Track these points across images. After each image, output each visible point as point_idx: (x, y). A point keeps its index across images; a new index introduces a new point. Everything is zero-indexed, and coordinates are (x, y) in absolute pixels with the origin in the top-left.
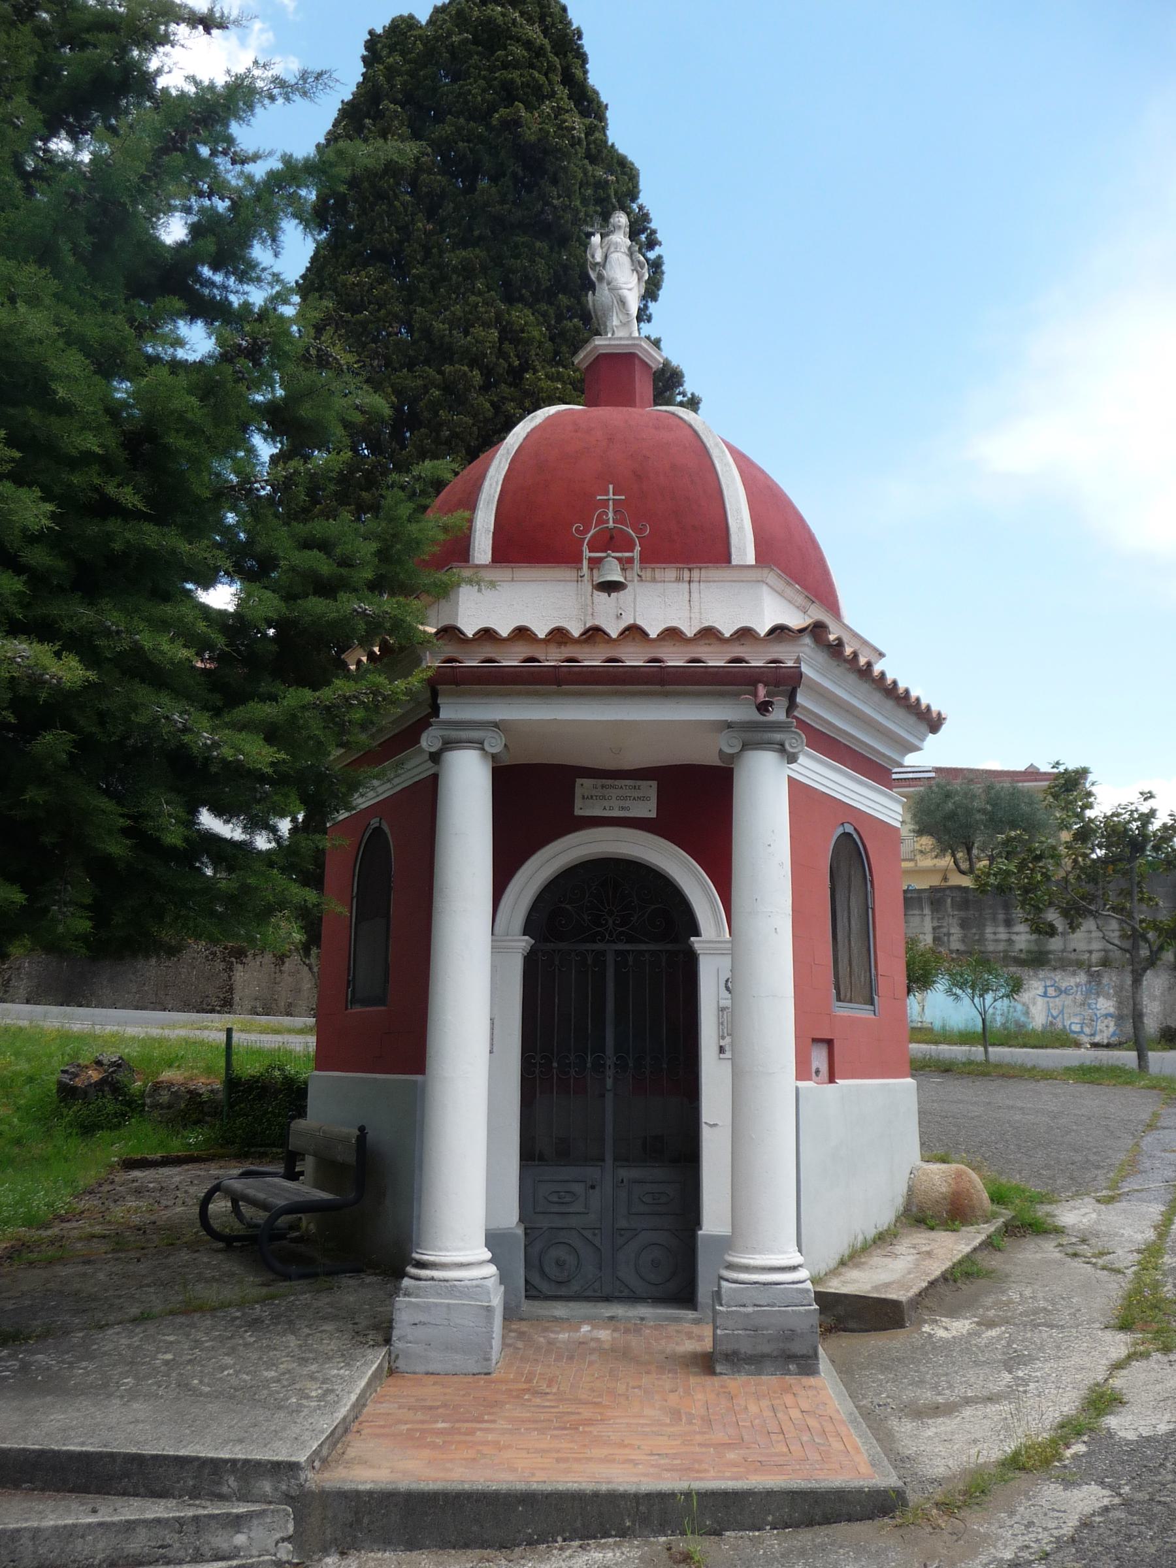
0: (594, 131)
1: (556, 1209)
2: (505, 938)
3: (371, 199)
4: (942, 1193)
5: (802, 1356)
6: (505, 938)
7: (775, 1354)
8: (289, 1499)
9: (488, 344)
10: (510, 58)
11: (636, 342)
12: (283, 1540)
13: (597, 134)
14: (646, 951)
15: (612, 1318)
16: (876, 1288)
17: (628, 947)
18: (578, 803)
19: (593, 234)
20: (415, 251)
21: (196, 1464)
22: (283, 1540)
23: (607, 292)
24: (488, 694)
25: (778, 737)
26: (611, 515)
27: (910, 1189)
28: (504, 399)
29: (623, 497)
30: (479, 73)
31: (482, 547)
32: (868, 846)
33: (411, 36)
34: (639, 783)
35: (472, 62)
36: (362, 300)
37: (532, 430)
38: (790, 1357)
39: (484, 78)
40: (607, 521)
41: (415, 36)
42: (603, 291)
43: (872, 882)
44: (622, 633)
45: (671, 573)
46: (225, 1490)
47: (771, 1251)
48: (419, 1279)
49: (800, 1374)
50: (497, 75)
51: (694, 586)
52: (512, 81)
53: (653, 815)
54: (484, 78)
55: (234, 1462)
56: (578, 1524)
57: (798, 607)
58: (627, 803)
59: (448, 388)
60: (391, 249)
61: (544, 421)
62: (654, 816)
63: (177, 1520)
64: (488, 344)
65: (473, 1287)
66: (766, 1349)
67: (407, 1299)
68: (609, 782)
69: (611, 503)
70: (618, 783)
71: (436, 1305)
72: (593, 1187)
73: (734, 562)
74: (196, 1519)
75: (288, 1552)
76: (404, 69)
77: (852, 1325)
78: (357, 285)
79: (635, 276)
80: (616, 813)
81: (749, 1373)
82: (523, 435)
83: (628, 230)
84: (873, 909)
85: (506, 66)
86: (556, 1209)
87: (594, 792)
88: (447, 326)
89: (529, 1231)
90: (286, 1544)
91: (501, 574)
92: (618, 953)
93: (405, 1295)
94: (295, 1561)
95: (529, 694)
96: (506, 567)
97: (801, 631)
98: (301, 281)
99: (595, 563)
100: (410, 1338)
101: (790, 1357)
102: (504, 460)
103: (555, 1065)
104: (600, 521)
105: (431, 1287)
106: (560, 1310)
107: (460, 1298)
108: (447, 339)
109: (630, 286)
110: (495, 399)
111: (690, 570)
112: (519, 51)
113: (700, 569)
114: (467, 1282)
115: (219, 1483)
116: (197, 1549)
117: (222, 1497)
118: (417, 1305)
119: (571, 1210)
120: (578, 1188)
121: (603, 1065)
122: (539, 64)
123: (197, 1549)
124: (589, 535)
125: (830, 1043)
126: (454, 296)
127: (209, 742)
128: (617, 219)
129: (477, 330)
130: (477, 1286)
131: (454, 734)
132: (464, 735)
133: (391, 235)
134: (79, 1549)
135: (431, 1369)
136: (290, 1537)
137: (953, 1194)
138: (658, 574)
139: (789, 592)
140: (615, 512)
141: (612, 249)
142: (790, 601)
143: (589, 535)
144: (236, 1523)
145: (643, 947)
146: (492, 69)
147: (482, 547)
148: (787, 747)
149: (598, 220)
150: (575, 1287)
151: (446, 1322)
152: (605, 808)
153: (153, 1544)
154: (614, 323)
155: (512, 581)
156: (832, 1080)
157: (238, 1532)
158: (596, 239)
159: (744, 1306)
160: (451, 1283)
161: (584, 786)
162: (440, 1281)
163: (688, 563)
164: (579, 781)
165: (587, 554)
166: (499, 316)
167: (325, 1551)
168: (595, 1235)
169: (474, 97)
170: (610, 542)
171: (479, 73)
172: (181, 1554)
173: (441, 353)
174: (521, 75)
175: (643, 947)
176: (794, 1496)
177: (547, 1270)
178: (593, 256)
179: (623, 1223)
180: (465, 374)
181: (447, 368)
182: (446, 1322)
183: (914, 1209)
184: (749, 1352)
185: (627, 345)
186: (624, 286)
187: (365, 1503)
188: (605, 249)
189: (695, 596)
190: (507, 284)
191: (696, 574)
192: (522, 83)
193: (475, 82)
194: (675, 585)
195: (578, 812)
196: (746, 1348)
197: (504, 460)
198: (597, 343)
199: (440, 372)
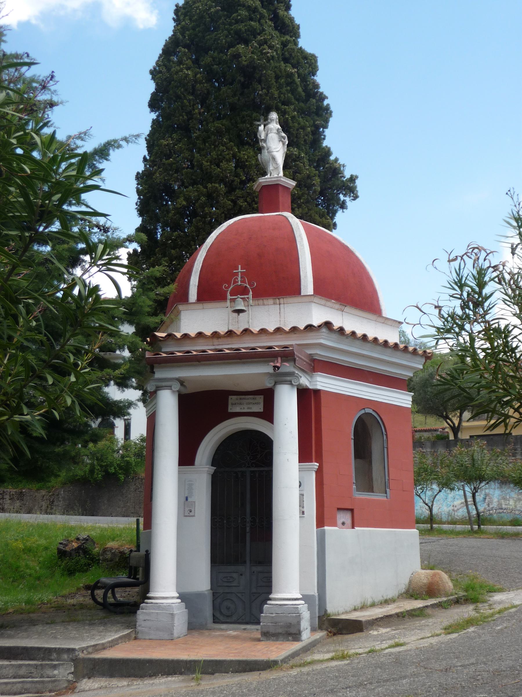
0: (288, 44)
1: (226, 584)
2: (200, 467)
3: (174, 98)
4: (424, 583)
5: (294, 634)
6: (200, 467)
7: (284, 633)
8: (73, 660)
9: (228, 171)
10: (239, 17)
11: (279, 179)
12: (70, 673)
13: (290, 46)
14: (263, 471)
15: (245, 629)
16: (356, 617)
17: (256, 469)
18: (230, 407)
19: (260, 125)
20: (195, 124)
21: (44, 649)
22: (70, 673)
23: (267, 154)
24: (173, 367)
25: (288, 378)
26: (239, 279)
27: (410, 582)
28: (238, 198)
29: (245, 271)
30: (224, 27)
31: (193, 294)
32: (383, 417)
33: (194, 7)
34: (256, 396)
35: (221, 21)
36: (170, 152)
37: (220, 234)
38: (290, 634)
39: (227, 29)
40: (238, 282)
41: (196, 7)
42: (265, 152)
43: (387, 435)
44: (242, 332)
45: (271, 301)
46: (53, 657)
47: (284, 592)
48: (147, 603)
49: (293, 641)
50: (233, 27)
51: (282, 306)
52: (240, 30)
53: (262, 410)
54: (227, 29)
55: (55, 649)
56: (166, 670)
57: (337, 309)
58: (250, 406)
59: (209, 196)
60: (184, 124)
61: (227, 228)
62: (262, 411)
63: (35, 665)
64: (228, 171)
65: (167, 606)
66: (280, 631)
67: (142, 611)
68: (243, 397)
69: (240, 274)
70: (247, 397)
71: (152, 613)
72: (241, 575)
73: (302, 294)
74: (41, 665)
75: (72, 678)
76: (191, 26)
77: (344, 632)
78: (167, 145)
79: (281, 143)
80: (246, 410)
81: (273, 640)
82: (215, 237)
83: (278, 120)
84: (387, 448)
85: (237, 22)
86: (226, 584)
87: (237, 402)
88: (209, 163)
89: (215, 594)
90: (71, 675)
91: (200, 306)
92: (252, 472)
93: (142, 609)
94: (74, 680)
95: (189, 366)
96: (200, 303)
97: (319, 326)
98: (148, 138)
99: (233, 301)
100: (143, 625)
101: (290, 634)
102: (204, 251)
103: (225, 522)
104: (235, 282)
105: (151, 606)
106: (224, 626)
107: (162, 610)
108: (209, 171)
109: (277, 150)
110: (234, 198)
111: (279, 299)
112: (244, 13)
113: (283, 298)
114: (165, 604)
115: (51, 655)
116: (42, 674)
117: (52, 660)
118: (145, 613)
119: (232, 585)
120: (235, 575)
121: (251, 522)
122: (254, 17)
123: (42, 674)
124: (230, 289)
125: (352, 510)
126: (213, 147)
127: (42, 400)
128: (271, 116)
129: (224, 164)
130: (169, 606)
131: (160, 384)
132: (164, 384)
133: (183, 117)
134: (4, 672)
135: (151, 638)
136: (73, 673)
137: (429, 583)
138: (265, 302)
139: (329, 304)
140: (241, 277)
141: (269, 132)
142: (331, 308)
143: (230, 289)
144: (55, 667)
145: (262, 469)
146: (231, 24)
147: (193, 294)
148: (293, 383)
149: (262, 118)
150: (234, 618)
151: (156, 620)
152: (241, 409)
153: (27, 672)
154: (271, 169)
155: (203, 309)
156: (353, 527)
157: (55, 670)
158: (261, 128)
159: (272, 614)
160: (159, 605)
161: (232, 399)
162: (155, 604)
163: (278, 296)
164: (230, 397)
165: (229, 297)
166: (234, 156)
167: (84, 677)
168: (242, 595)
169: (222, 41)
170: (242, 291)
171: (224, 27)
172: (37, 675)
173: (208, 177)
174: (245, 26)
175: (262, 469)
176: (239, 662)
177: (222, 611)
178: (260, 136)
179: (254, 590)
180: (217, 188)
181: (209, 185)
182: (156, 620)
183: (411, 591)
184: (273, 632)
185: (275, 181)
186: (274, 150)
187: (97, 662)
188: (266, 132)
189: (282, 310)
190: (239, 136)
191: (282, 301)
192: (245, 29)
193: (223, 32)
194: (273, 306)
195: (230, 411)
196: (272, 630)
197: (204, 251)
198: (260, 181)
199: (206, 187)
